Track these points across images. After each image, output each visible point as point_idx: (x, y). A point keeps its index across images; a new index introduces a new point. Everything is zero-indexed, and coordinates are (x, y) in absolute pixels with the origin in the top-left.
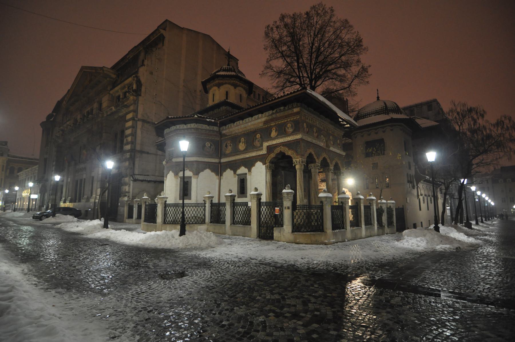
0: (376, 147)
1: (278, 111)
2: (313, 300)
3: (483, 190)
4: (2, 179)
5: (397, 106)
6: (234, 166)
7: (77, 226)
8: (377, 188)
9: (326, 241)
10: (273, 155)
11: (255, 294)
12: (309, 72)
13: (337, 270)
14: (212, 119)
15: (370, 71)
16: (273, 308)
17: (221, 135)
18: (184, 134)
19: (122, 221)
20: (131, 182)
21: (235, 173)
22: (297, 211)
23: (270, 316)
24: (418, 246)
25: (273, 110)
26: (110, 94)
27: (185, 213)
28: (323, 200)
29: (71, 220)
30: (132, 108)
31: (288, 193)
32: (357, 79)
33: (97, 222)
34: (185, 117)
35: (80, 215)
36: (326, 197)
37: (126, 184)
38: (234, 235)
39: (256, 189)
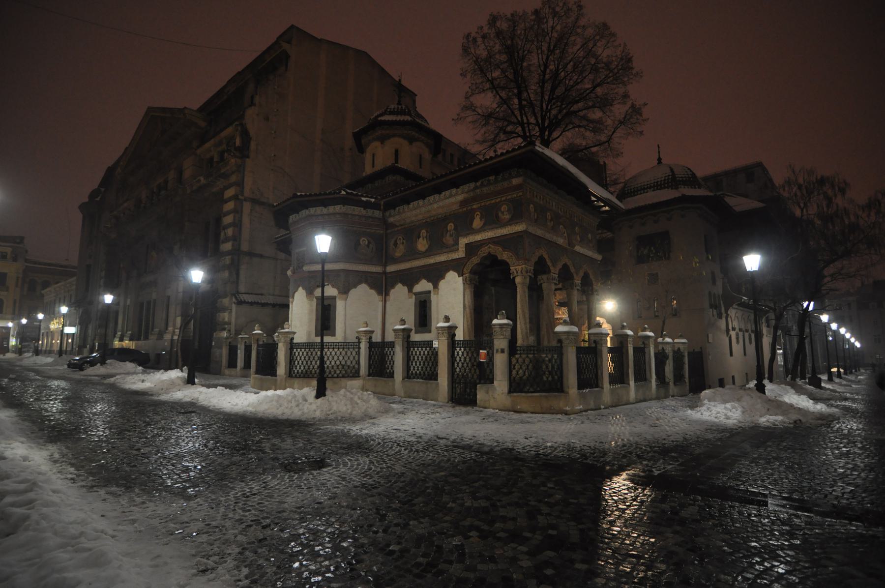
0: (654, 246)
2: (545, 509)
3: (841, 322)
5: (694, 175)
6: (409, 279)
7: (143, 381)
9: (568, 408)
10: (475, 260)
11: (445, 498)
12: (539, 115)
13: (586, 459)
14: (372, 197)
16: (477, 523)
17: (388, 226)
18: (323, 225)
19: (218, 373)
20: (234, 306)
21: (410, 290)
22: (517, 356)
23: (471, 537)
24: (728, 418)
25: (476, 181)
27: (325, 359)
28: (563, 337)
29: (133, 370)
30: (233, 178)
31: (501, 326)
32: (623, 127)
33: (175, 374)
34: (325, 194)
35: (150, 362)
37: (224, 309)
38: (410, 397)
39: (447, 319)
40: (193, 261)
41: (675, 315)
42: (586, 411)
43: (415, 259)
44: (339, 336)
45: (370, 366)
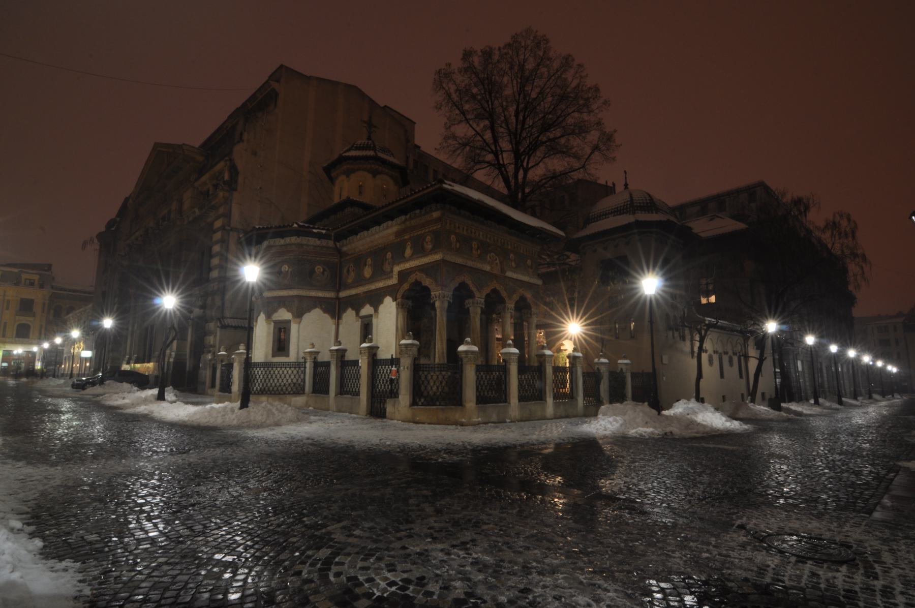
4: (5, 323)
5: (651, 199)
6: (356, 304)
7: (124, 398)
8: (617, 338)
10: (406, 286)
19: (203, 393)
25: (406, 214)
28: (463, 356)
30: (221, 210)
31: (406, 345)
32: (596, 153)
35: (142, 382)
36: (466, 352)
38: (340, 411)
40: (159, 288)
41: (632, 337)
42: (486, 423)
45: (314, 383)
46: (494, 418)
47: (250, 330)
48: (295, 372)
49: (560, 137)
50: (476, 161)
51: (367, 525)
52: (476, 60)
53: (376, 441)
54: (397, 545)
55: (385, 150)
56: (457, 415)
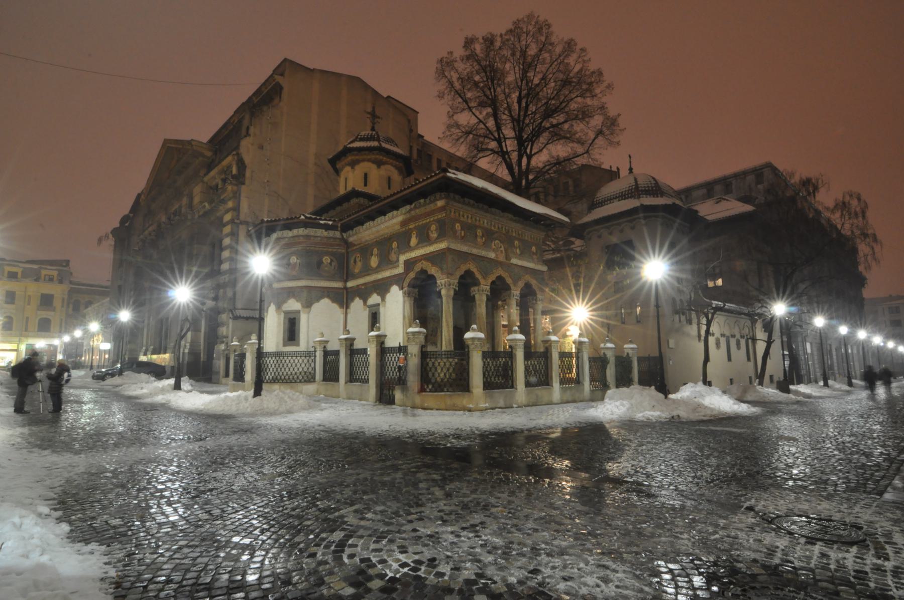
1: (418, 205)
4: (27, 318)
7: (142, 388)
8: (623, 323)
9: (471, 406)
10: (412, 275)
15: (622, 122)
17: (347, 244)
19: (218, 383)
25: (411, 204)
26: (203, 182)
28: (470, 342)
30: (230, 204)
31: (414, 333)
32: (600, 138)
35: (158, 372)
36: (473, 339)
37: (223, 324)
38: (350, 399)
40: (174, 281)
41: (638, 322)
43: (368, 275)
44: (303, 346)
45: (325, 372)
46: (501, 403)
47: (261, 320)
48: (306, 361)
49: (563, 123)
50: (479, 149)
51: (379, 508)
52: (478, 48)
53: (385, 427)
54: (408, 527)
55: (389, 141)
56: (462, 400)
